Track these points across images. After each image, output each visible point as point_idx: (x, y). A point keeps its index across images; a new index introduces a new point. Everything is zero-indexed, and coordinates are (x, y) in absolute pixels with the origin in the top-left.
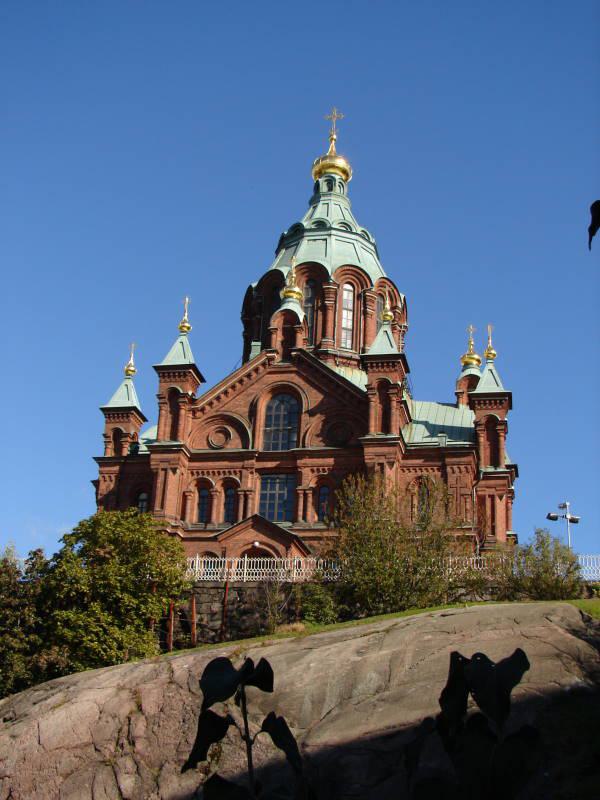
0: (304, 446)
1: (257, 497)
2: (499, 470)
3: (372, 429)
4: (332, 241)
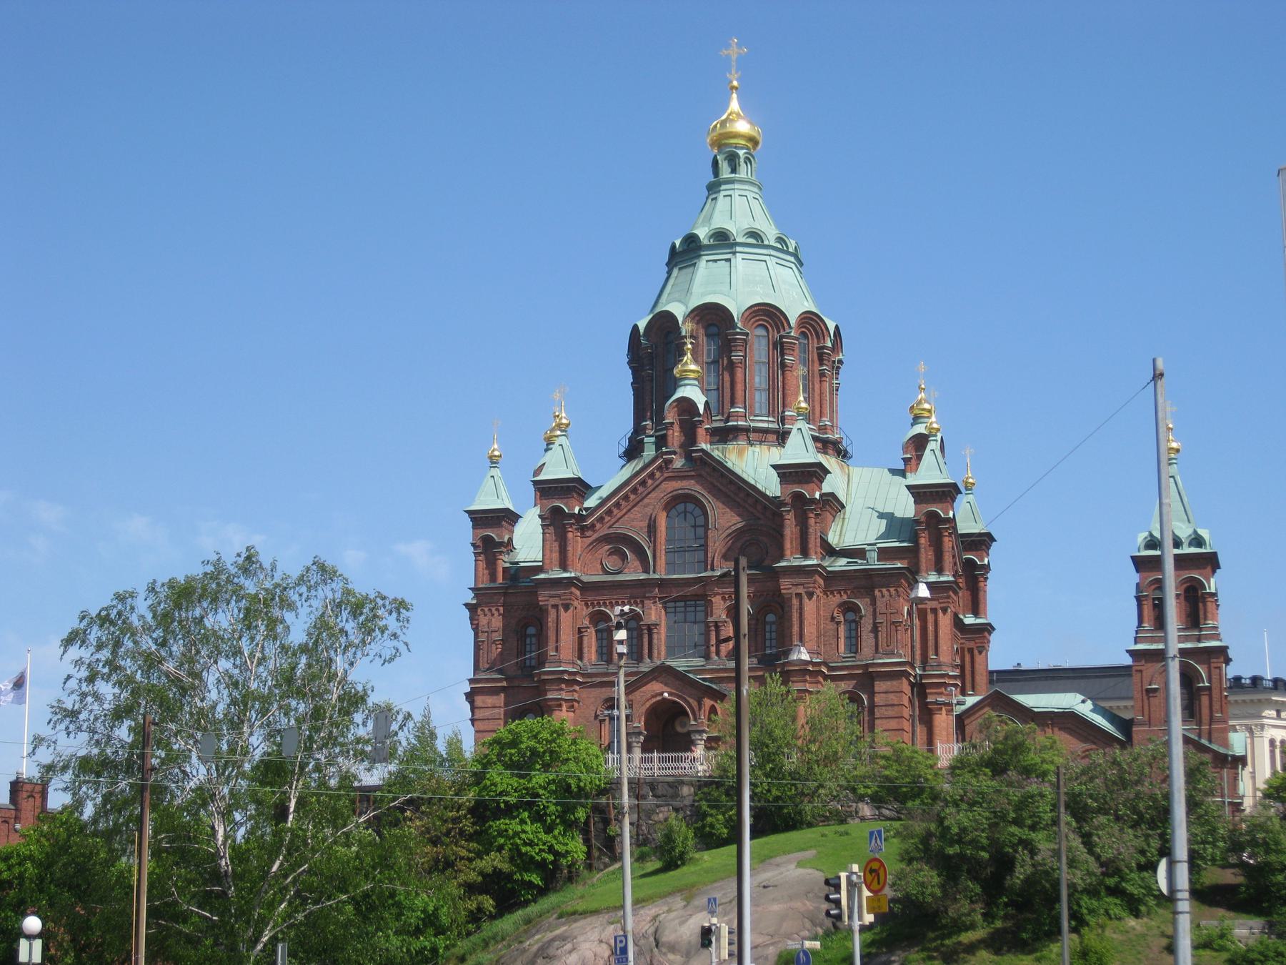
0: (713, 569)
1: (663, 630)
2: (943, 579)
3: (788, 552)
4: (738, 260)
